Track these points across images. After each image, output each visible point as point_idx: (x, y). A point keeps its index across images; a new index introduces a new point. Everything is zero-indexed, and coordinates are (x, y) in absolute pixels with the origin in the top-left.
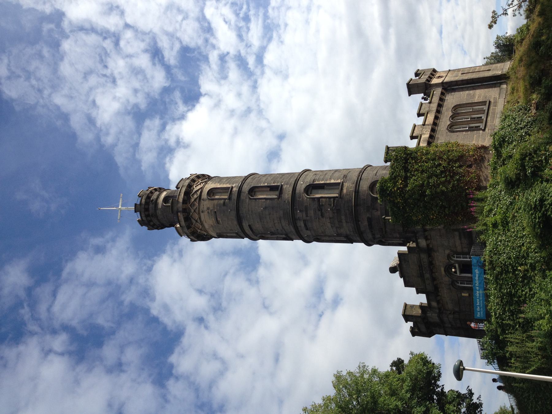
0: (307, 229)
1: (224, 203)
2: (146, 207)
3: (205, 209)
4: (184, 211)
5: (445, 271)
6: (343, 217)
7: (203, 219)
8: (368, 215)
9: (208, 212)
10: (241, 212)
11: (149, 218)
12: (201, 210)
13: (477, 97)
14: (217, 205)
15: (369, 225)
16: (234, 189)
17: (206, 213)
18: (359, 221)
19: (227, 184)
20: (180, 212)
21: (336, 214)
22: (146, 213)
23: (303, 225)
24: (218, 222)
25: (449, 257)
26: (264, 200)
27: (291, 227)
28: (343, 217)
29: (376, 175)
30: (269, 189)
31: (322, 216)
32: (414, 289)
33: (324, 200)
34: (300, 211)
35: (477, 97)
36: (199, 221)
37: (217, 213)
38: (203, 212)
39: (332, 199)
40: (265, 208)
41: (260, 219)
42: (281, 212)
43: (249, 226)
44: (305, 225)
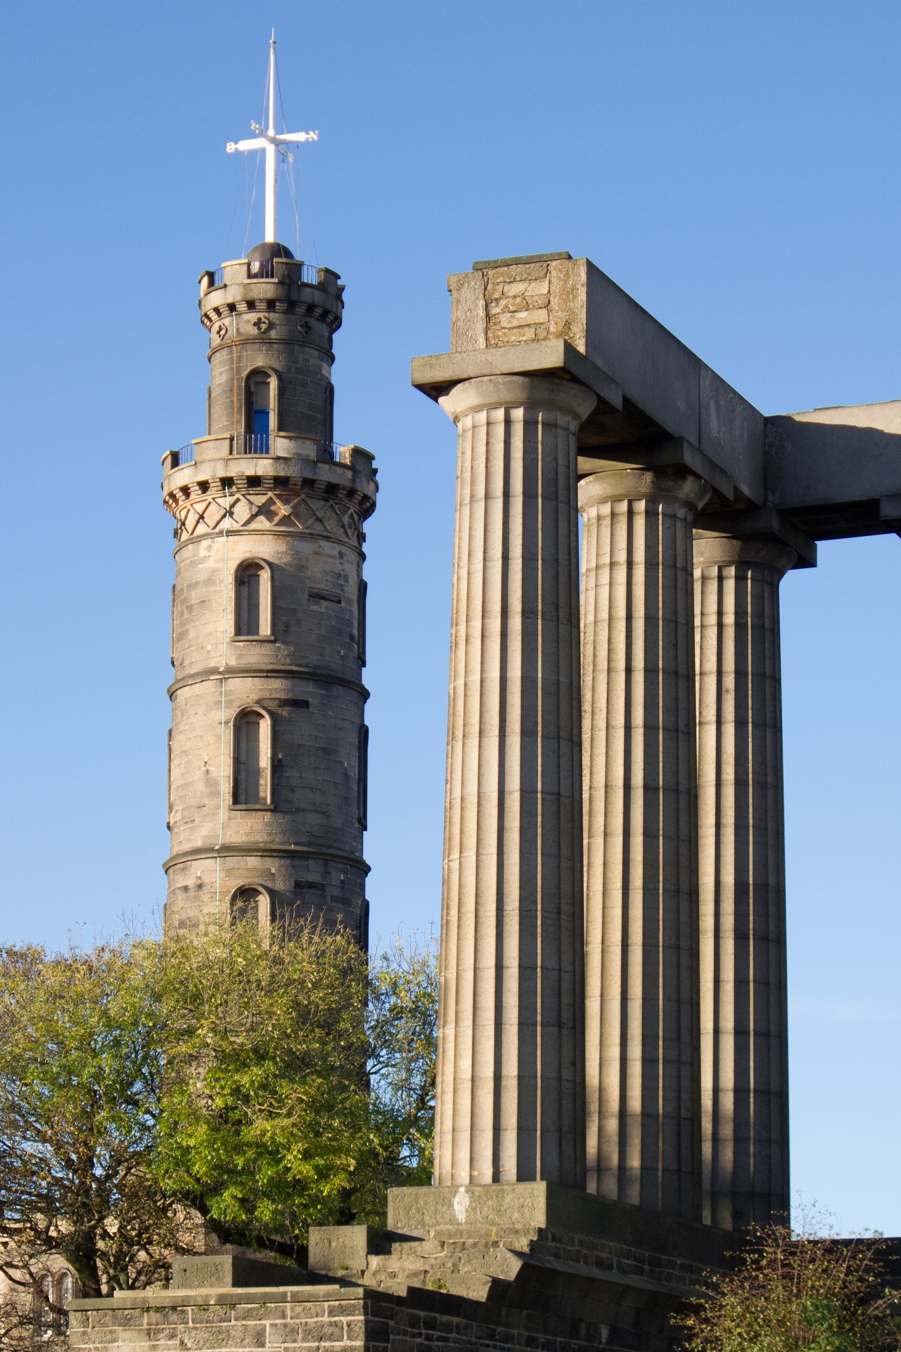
0: (298, 885)
4: (352, 493)
7: (328, 547)
9: (339, 575)
11: (301, 310)
12: (345, 550)
14: (351, 612)
20: (354, 481)
22: (318, 311)
24: (317, 596)
27: (304, 839)
34: (342, 881)
36: (318, 528)
38: (341, 555)
40: (347, 776)
41: (324, 749)
43: (305, 704)
44: (311, 885)
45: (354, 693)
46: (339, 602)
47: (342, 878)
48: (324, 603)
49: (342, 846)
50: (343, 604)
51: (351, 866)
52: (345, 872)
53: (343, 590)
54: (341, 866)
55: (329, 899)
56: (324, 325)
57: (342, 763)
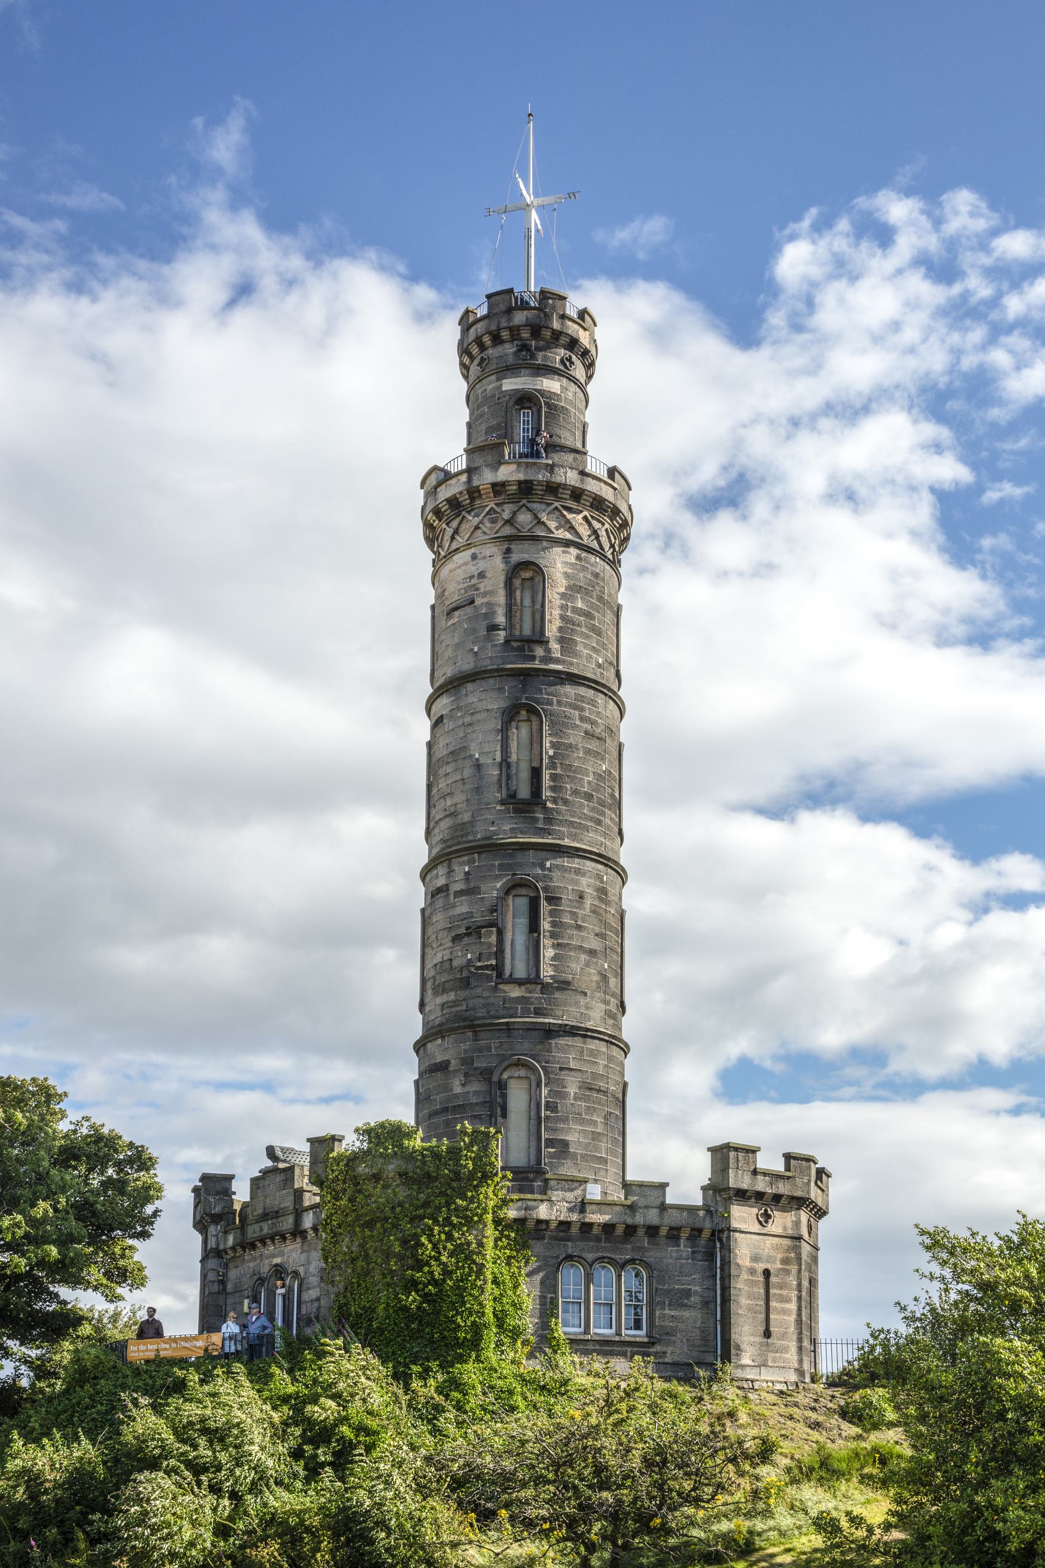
1: (493, 628)
2: (505, 334)
3: (482, 565)
4: (474, 493)
5: (277, 1265)
6: (452, 996)
8: (454, 1064)
10: (470, 687)
13: (673, 1313)
15: (435, 1064)
16: (539, 651)
17: (473, 570)
18: (443, 1038)
19: (563, 618)
21: (458, 976)
22: (487, 340)
23: (441, 882)
25: (296, 1274)
26: (498, 759)
28: (452, 996)
29: (561, 1069)
30: (536, 764)
31: (457, 939)
32: (248, 1199)
33: (493, 939)
34: (467, 874)
35: (673, 1313)
36: (454, 546)
37: (468, 610)
39: (494, 962)
40: (478, 766)
41: (452, 753)
42: (466, 817)
45: (491, 681)
46: (472, 602)
47: (467, 869)
48: (457, 613)
49: (471, 838)
50: (479, 601)
51: (479, 853)
52: (469, 863)
53: (477, 589)
54: (466, 858)
55: (452, 897)
56: (507, 346)
57: (471, 756)
